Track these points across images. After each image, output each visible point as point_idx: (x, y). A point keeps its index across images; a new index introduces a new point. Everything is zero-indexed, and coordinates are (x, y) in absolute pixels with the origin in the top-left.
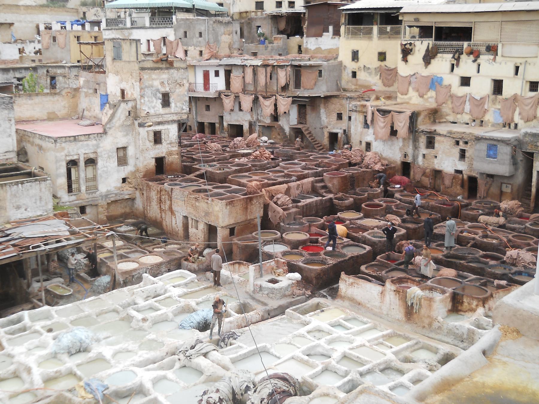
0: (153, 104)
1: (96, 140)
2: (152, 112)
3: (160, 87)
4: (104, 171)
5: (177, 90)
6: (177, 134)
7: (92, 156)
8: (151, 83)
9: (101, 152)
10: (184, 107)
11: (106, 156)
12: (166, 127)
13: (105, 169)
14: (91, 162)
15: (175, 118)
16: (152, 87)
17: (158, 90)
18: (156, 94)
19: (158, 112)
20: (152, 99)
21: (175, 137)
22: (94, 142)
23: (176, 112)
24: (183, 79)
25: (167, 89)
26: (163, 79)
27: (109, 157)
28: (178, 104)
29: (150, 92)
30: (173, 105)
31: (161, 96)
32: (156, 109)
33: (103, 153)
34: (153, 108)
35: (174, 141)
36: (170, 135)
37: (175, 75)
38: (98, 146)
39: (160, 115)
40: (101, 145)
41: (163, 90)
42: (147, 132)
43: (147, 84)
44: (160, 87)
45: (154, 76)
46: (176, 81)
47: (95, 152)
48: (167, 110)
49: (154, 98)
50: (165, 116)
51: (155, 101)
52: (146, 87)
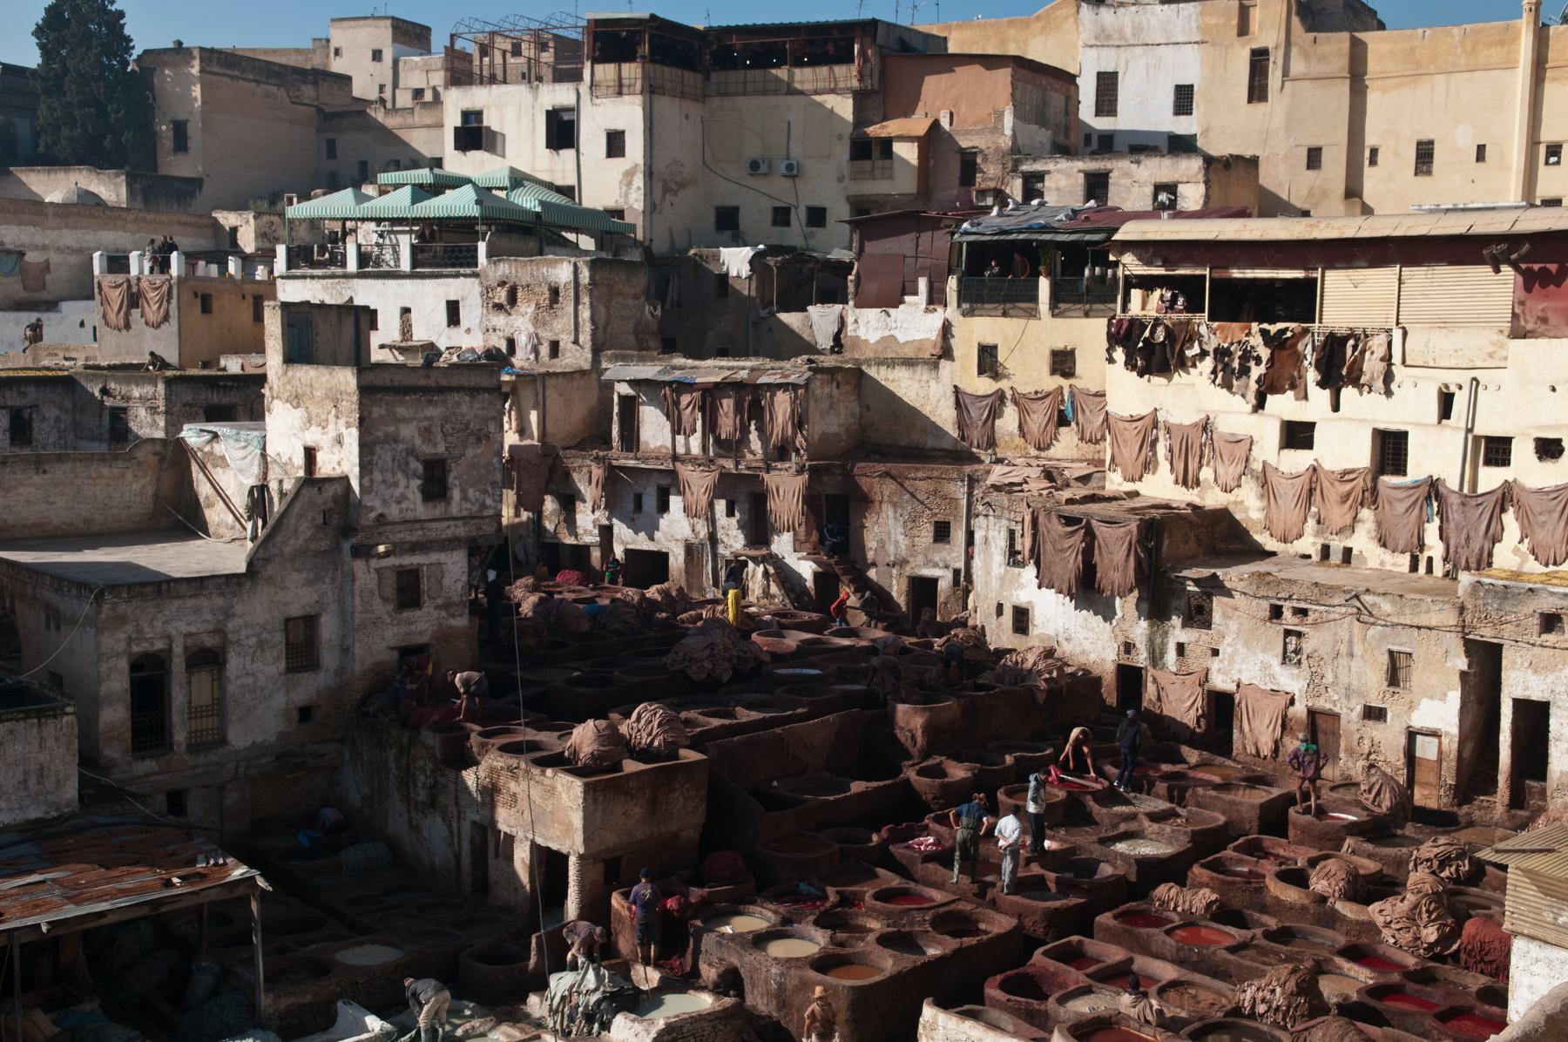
0: (398, 492)
2: (394, 512)
3: (418, 441)
6: (465, 578)
7: (209, 641)
8: (391, 429)
10: (489, 502)
12: (434, 557)
14: (208, 659)
15: (462, 531)
17: (411, 451)
18: (407, 463)
19: (410, 515)
20: (394, 474)
21: (459, 585)
22: (220, 602)
26: (431, 419)
28: (471, 491)
29: (389, 457)
30: (456, 494)
32: (404, 505)
33: (244, 633)
34: (399, 502)
36: (446, 582)
39: (417, 521)
40: (239, 609)
41: (427, 450)
42: (378, 571)
43: (380, 434)
45: (401, 411)
47: (220, 631)
48: (438, 510)
49: (400, 475)
51: (403, 482)
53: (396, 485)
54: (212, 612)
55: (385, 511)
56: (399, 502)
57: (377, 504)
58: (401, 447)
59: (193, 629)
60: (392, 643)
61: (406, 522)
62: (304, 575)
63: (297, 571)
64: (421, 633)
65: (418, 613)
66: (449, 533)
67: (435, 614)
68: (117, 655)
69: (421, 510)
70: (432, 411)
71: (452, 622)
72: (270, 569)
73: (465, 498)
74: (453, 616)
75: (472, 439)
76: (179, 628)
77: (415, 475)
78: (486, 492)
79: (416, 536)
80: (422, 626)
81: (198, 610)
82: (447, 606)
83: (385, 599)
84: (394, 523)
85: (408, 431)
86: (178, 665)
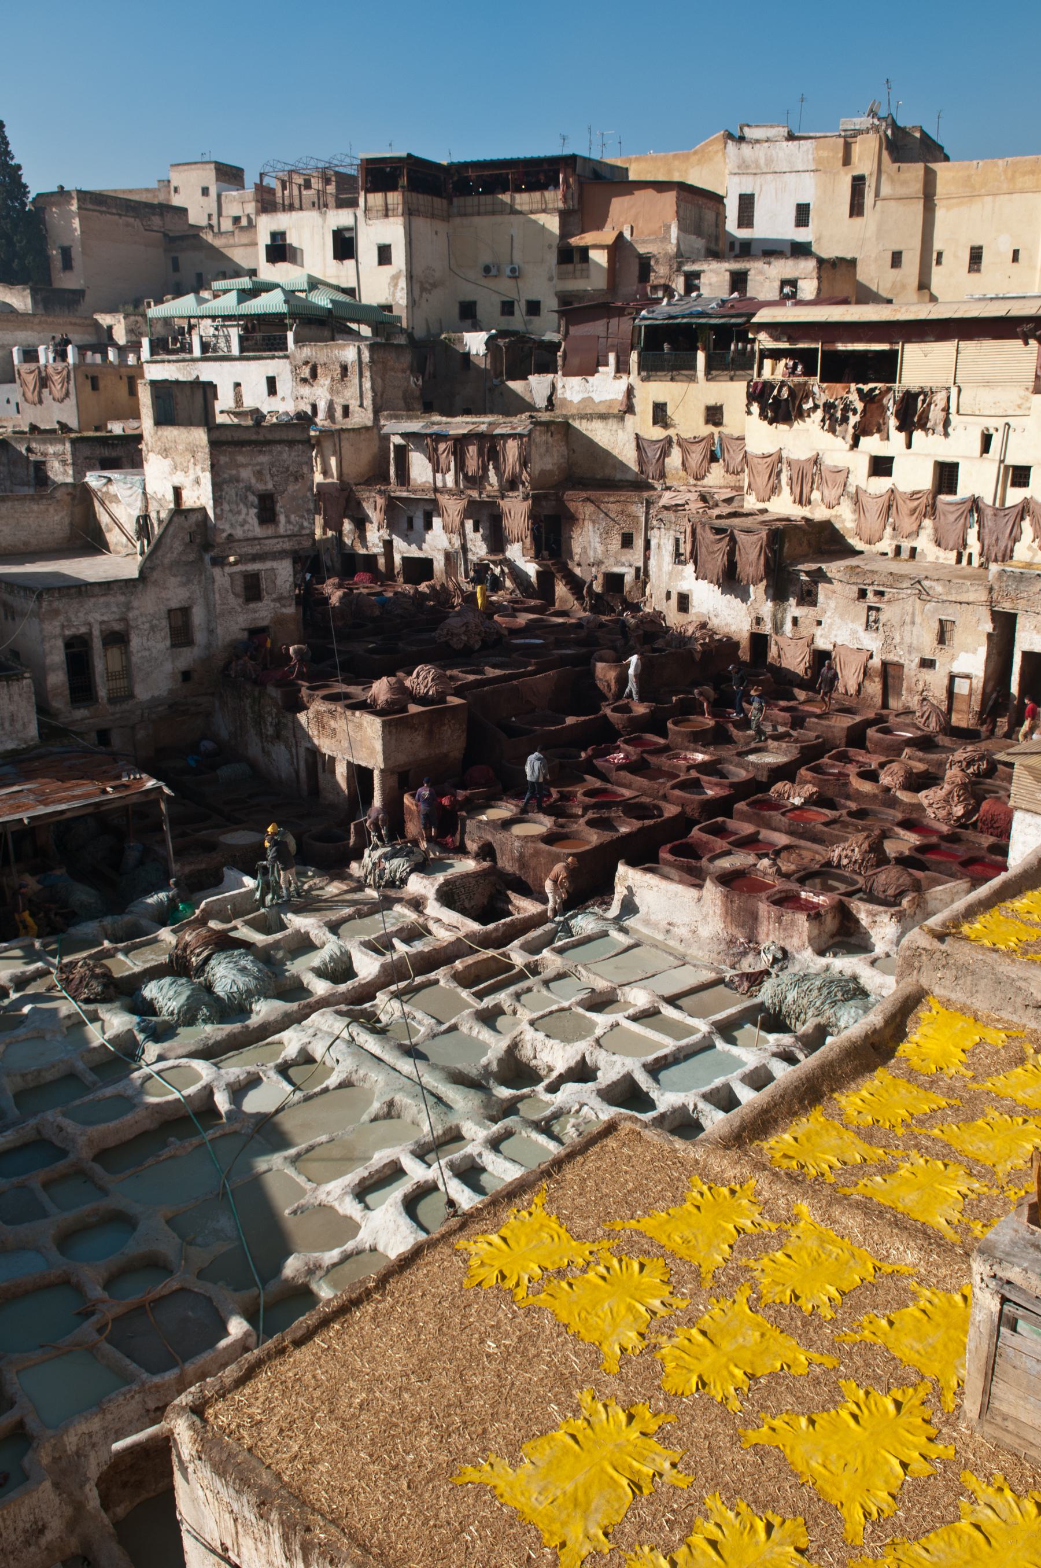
0: (241, 518)
1: (123, 594)
2: (239, 533)
3: (253, 481)
4: (142, 657)
5: (291, 488)
6: (291, 579)
7: (117, 627)
8: (234, 472)
9: (136, 619)
10: (306, 524)
11: (147, 626)
12: (269, 564)
13: (147, 653)
14: (117, 639)
15: (287, 545)
16: (238, 481)
17: (249, 488)
18: (246, 497)
19: (250, 535)
20: (238, 505)
21: (288, 584)
22: (122, 599)
24: (300, 464)
26: (261, 464)
27: (153, 628)
28: (293, 517)
29: (233, 492)
30: (282, 519)
31: (256, 500)
32: (246, 527)
33: (140, 620)
34: (242, 525)
36: (279, 582)
37: (285, 456)
38: (129, 607)
39: (255, 539)
40: (136, 604)
41: (260, 487)
42: (231, 575)
43: (226, 476)
44: (253, 481)
45: (240, 459)
46: (288, 469)
47: (124, 619)
48: (270, 531)
49: (241, 506)
50: (267, 542)
51: (244, 511)
52: (225, 482)
53: (239, 513)
54: (118, 605)
55: (233, 532)
56: (242, 525)
57: (227, 527)
58: (241, 485)
59: (105, 618)
60: (243, 626)
61: (248, 540)
62: (179, 579)
63: (175, 576)
64: (263, 619)
65: (260, 604)
66: (278, 547)
67: (272, 605)
68: (55, 637)
69: (258, 531)
70: (263, 459)
71: (284, 610)
72: (155, 575)
73: (289, 522)
74: (284, 606)
75: (291, 479)
76: (96, 617)
77: (253, 506)
78: (303, 517)
79: (256, 549)
80: (264, 614)
81: (107, 605)
82: (280, 599)
83: (236, 595)
84: (239, 541)
85: (246, 474)
86: (97, 644)
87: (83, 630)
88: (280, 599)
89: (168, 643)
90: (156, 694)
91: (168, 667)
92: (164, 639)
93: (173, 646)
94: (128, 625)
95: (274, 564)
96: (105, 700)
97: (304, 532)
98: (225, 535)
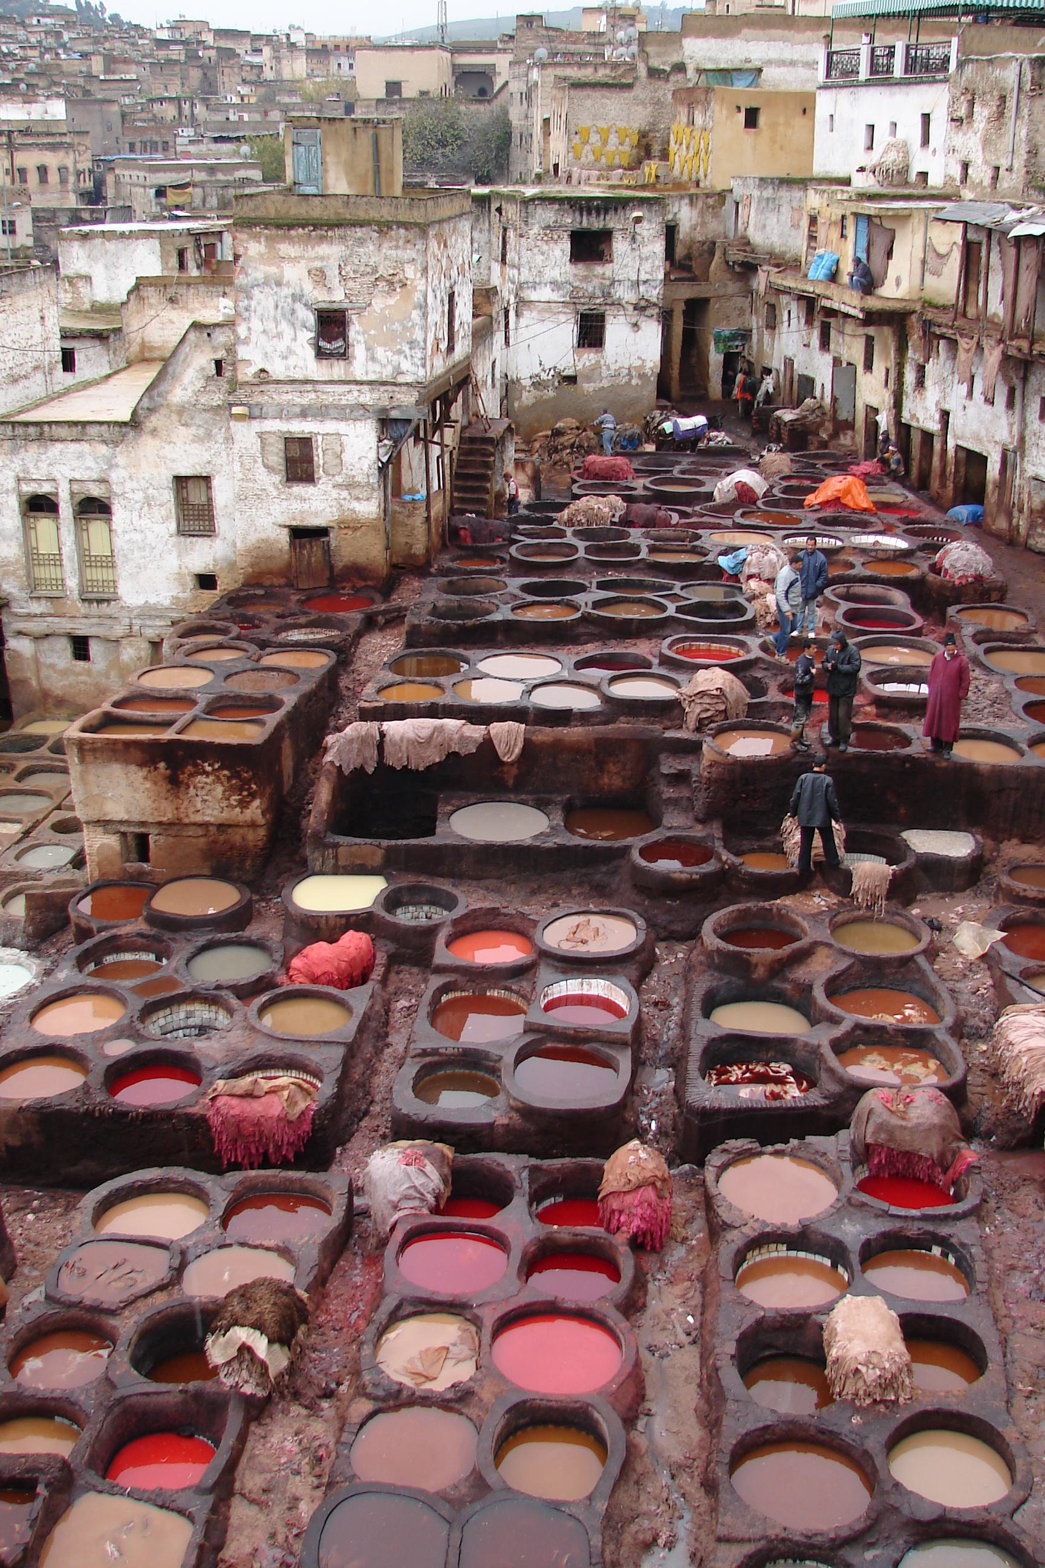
0: (282, 346)
2: (278, 370)
3: (308, 286)
5: (378, 304)
7: (96, 491)
10: (405, 365)
11: (139, 496)
12: (330, 426)
13: (138, 537)
14: (94, 508)
15: (367, 397)
19: (299, 375)
23: (372, 377)
25: (338, 296)
26: (322, 259)
27: (148, 502)
28: (380, 352)
30: (359, 351)
31: (311, 319)
32: (292, 361)
33: (129, 485)
35: (359, 478)
39: (306, 382)
41: (322, 297)
45: (286, 249)
46: (375, 270)
47: (103, 481)
48: (338, 369)
49: (284, 326)
53: (279, 335)
54: (95, 459)
58: (286, 291)
61: (293, 382)
62: (193, 430)
63: (186, 425)
67: (335, 493)
70: (324, 249)
72: (154, 421)
74: (358, 499)
78: (400, 352)
81: (80, 456)
82: (350, 485)
84: (278, 382)
87: (46, 488)
88: (350, 485)
89: (173, 527)
90: (153, 600)
91: (172, 563)
92: (165, 519)
93: (181, 532)
94: (110, 490)
95: (341, 427)
96: (76, 595)
97: (401, 379)
98: (252, 371)
